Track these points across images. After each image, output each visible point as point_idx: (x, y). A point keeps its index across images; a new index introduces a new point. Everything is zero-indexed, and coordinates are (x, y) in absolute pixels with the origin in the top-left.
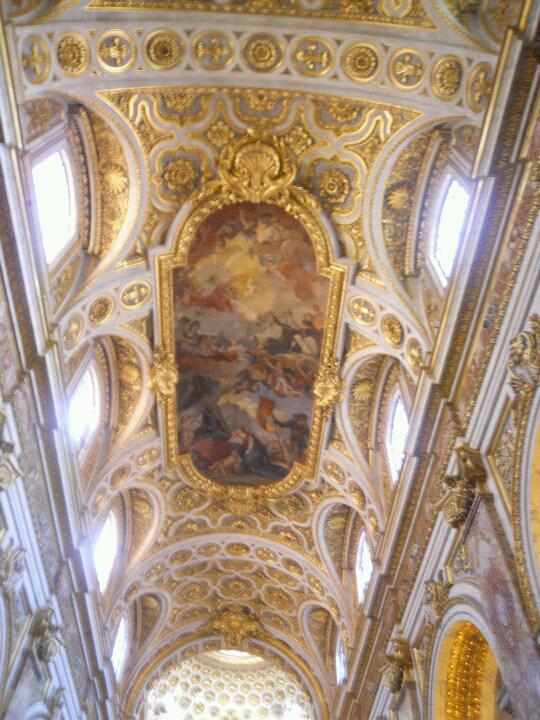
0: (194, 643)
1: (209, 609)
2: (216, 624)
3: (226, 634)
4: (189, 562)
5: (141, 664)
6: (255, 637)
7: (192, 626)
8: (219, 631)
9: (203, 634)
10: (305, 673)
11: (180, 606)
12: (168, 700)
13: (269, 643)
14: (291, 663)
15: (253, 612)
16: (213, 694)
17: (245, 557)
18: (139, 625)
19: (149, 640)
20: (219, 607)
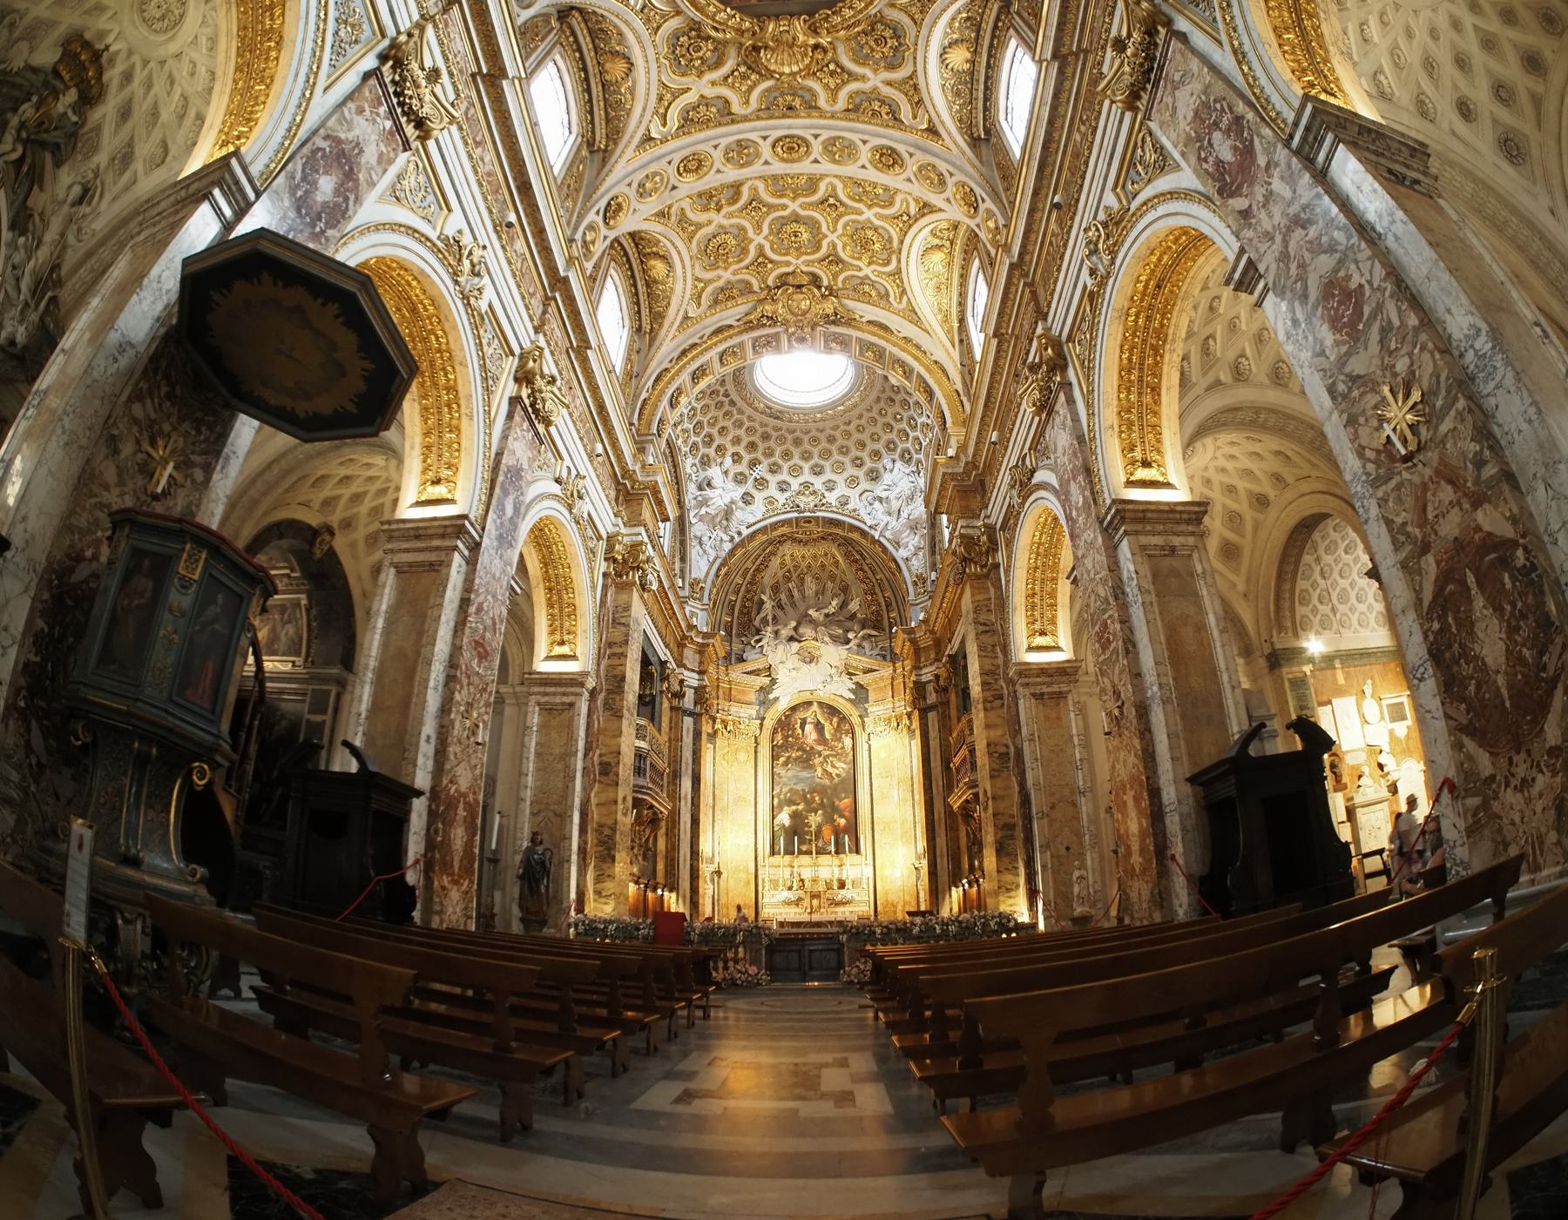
0: (736, 340)
1: (756, 288)
2: (768, 308)
3: (785, 323)
4: (710, 181)
5: (654, 369)
6: (833, 323)
7: (731, 314)
8: (773, 320)
9: (749, 326)
10: (916, 358)
11: (708, 275)
12: (714, 473)
13: (859, 329)
14: (895, 350)
15: (825, 283)
16: (780, 467)
17: (805, 167)
18: (645, 312)
19: (663, 332)
20: (770, 282)
